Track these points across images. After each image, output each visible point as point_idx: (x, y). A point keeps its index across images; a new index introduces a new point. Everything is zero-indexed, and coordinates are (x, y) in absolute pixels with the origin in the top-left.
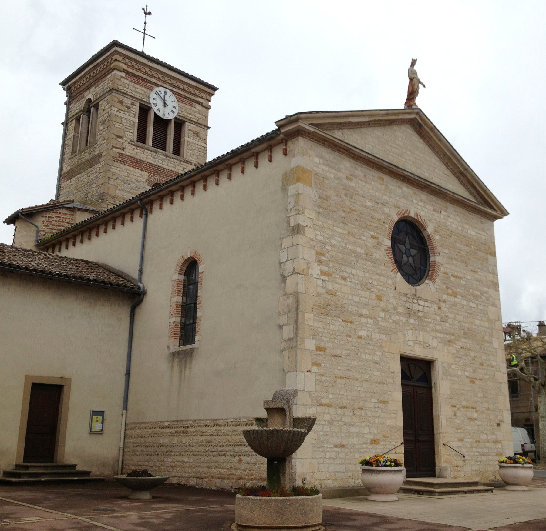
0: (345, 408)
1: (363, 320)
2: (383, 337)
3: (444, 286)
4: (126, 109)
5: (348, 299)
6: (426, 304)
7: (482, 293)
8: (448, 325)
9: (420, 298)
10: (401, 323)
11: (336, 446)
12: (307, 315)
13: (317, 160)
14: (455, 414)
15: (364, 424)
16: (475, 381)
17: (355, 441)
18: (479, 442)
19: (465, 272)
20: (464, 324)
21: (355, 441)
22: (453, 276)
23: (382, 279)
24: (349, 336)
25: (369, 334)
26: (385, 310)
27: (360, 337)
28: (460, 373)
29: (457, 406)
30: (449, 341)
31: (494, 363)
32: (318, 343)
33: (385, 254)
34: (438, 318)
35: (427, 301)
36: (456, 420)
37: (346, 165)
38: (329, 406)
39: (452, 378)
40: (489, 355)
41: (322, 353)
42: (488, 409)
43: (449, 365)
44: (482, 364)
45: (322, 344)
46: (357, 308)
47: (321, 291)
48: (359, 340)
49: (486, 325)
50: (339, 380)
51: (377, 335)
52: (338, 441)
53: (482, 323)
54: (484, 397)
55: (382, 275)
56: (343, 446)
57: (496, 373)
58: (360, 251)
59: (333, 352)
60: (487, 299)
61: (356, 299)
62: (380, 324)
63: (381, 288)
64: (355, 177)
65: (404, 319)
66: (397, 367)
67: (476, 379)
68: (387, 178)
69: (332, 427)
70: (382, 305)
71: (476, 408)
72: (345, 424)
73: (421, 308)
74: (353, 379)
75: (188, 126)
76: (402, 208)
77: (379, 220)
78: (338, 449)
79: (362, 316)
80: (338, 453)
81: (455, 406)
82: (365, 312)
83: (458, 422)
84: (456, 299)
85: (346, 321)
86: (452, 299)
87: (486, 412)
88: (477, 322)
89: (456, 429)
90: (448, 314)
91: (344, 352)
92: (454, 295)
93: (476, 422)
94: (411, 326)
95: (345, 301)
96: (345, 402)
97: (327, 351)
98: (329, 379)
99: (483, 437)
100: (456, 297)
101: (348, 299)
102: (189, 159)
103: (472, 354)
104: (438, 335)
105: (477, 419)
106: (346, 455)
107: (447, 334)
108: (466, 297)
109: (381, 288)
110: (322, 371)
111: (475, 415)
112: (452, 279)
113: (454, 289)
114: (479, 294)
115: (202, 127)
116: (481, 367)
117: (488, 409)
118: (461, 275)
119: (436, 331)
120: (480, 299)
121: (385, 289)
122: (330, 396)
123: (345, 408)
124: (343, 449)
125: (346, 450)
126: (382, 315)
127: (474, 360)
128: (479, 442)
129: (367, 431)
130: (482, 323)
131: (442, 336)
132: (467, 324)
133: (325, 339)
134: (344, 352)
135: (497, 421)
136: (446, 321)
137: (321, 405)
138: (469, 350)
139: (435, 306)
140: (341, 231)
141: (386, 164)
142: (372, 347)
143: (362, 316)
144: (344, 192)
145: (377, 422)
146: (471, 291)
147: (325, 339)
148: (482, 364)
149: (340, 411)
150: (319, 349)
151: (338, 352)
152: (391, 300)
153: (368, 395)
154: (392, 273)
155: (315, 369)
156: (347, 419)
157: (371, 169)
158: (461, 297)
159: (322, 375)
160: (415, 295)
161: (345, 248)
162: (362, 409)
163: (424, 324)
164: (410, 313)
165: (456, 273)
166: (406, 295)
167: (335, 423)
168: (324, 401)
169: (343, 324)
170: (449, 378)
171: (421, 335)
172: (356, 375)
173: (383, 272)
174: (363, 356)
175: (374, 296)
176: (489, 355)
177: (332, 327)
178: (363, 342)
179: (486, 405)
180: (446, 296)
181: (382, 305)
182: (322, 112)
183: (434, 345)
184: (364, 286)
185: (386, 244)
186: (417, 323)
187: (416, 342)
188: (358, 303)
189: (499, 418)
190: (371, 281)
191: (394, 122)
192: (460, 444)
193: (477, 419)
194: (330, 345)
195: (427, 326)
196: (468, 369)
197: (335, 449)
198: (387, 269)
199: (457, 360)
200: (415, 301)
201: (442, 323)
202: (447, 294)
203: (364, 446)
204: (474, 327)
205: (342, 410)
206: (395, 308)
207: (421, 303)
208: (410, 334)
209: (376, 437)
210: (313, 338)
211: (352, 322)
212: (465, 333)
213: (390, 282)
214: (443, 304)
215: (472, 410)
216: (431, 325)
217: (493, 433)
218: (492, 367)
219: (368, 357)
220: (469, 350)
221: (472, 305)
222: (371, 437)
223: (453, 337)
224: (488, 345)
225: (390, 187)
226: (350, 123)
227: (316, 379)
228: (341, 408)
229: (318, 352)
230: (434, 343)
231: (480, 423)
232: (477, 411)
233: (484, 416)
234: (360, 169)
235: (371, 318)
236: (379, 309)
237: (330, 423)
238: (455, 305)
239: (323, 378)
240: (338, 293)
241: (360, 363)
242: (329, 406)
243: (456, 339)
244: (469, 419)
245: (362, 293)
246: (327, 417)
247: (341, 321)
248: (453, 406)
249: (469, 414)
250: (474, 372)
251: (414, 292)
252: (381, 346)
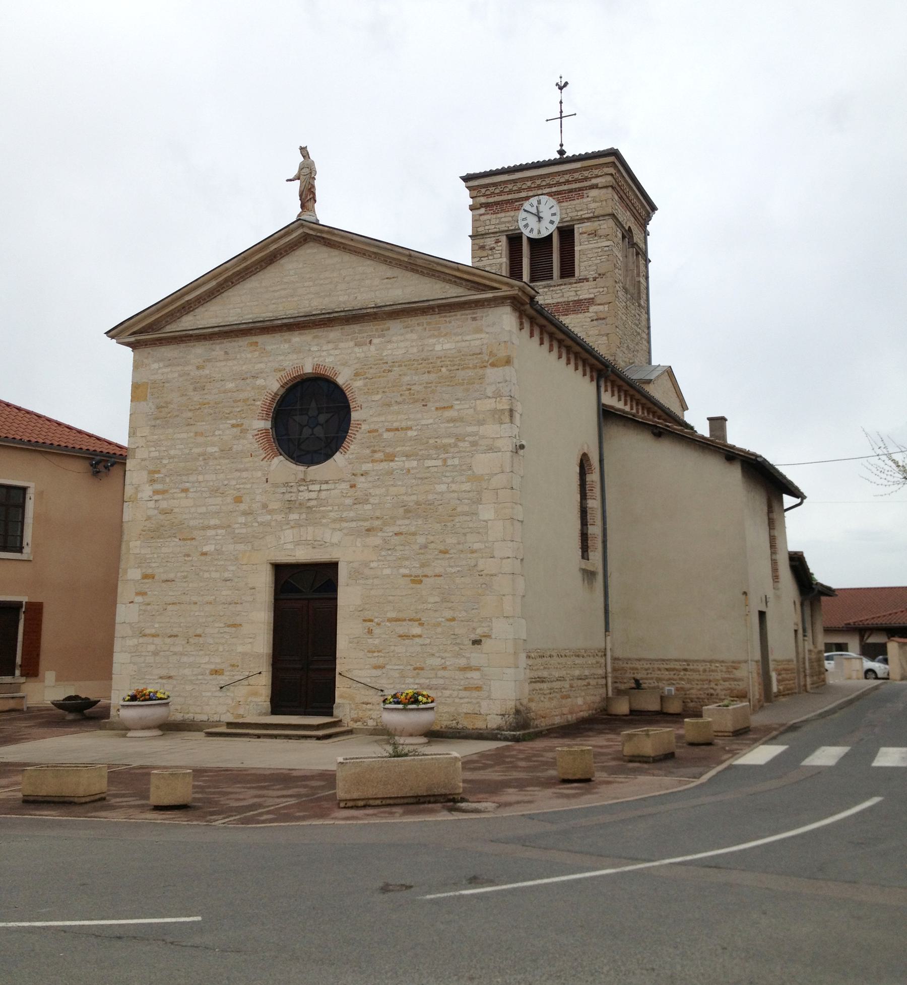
0: (176, 636)
1: (210, 533)
2: (241, 547)
3: (368, 451)
4: (490, 252)
5: (190, 513)
6: (324, 487)
7: (459, 438)
8: (369, 507)
9: (313, 482)
10: (273, 524)
11: (161, 678)
12: (132, 544)
13: (156, 366)
14: (370, 632)
15: (202, 652)
16: (424, 579)
17: (187, 671)
18: (422, 669)
19: (419, 416)
20: (405, 498)
21: (187, 671)
22: (388, 430)
23: (245, 474)
24: (188, 556)
25: (218, 547)
26: (245, 513)
27: (204, 554)
28: (387, 571)
29: (376, 620)
30: (368, 530)
31: (476, 546)
32: (144, 570)
33: (254, 440)
34: (348, 501)
35: (327, 482)
36: (370, 641)
37: (198, 351)
38: (154, 636)
39: (370, 581)
40: (465, 534)
41: (150, 580)
42: (453, 619)
43: (366, 564)
44: (445, 552)
45: (150, 571)
46: (201, 521)
47: (151, 512)
48: (203, 558)
49: (466, 487)
50: (170, 607)
51: (231, 547)
52: (164, 672)
53: (454, 487)
54: (444, 600)
55: (246, 470)
56: (170, 677)
57: (481, 563)
58: (210, 450)
59: (165, 577)
60: (474, 444)
61: (203, 510)
62: (237, 531)
63: (242, 486)
64: (209, 361)
65: (279, 517)
66: (264, 582)
67: (426, 576)
68: (261, 339)
69: (157, 658)
70: (243, 507)
71: (420, 620)
72: (175, 654)
73: (313, 495)
74: (190, 603)
75: (578, 229)
76: (287, 369)
77: (245, 401)
78: (164, 681)
79: (209, 527)
80: (164, 684)
81: (371, 621)
82: (213, 522)
83: (377, 642)
84: (392, 464)
85: (184, 539)
86: (385, 465)
87: (448, 624)
88: (442, 488)
89: (369, 651)
90: (371, 491)
91: (179, 574)
92: (390, 458)
93: (417, 640)
94: (292, 523)
95: (185, 516)
96: (175, 629)
97: (156, 577)
98: (156, 607)
99: (436, 662)
100: (392, 461)
101: (190, 513)
102: (584, 274)
103: (421, 540)
104: (345, 525)
105: (420, 636)
106: (175, 687)
107: (366, 520)
108: (417, 455)
109: (242, 486)
110: (147, 600)
111: (417, 630)
112: (386, 435)
113: (388, 450)
114: (452, 441)
115: (601, 218)
116: (441, 556)
117: (453, 619)
118: (409, 423)
119: (342, 520)
120: (452, 450)
121: (249, 486)
122: (157, 625)
123: (176, 636)
124: (170, 681)
125: (175, 682)
126: (242, 519)
127: (426, 547)
128: (422, 669)
129: (206, 659)
130: (454, 487)
131: (354, 524)
132: (414, 498)
133: (154, 565)
134: (179, 574)
135: (473, 637)
136: (366, 502)
137: (145, 635)
138: (414, 534)
139: (344, 486)
140: (184, 435)
141: (244, 326)
142: (222, 563)
143: (209, 527)
144: (192, 387)
145: (221, 649)
146: (431, 441)
147: (154, 565)
148: (445, 552)
149: (168, 640)
150: (145, 576)
151: (171, 576)
152: (258, 498)
153: (210, 619)
154: (264, 462)
155: (139, 599)
156: (178, 649)
157: (236, 339)
158: (404, 458)
159: (149, 604)
160: (304, 480)
161: (188, 454)
162: (200, 636)
163: (318, 515)
164: (291, 506)
165: (396, 425)
166: (286, 484)
167: (162, 653)
168: (147, 631)
169: (182, 543)
170: (361, 581)
171: (310, 533)
172: (194, 599)
173: (248, 465)
174: (206, 575)
175: (229, 500)
176: (465, 534)
177: (164, 550)
178: (208, 558)
179: (448, 614)
180: (370, 465)
181: (243, 507)
182: (137, 315)
183: (335, 540)
184: (215, 491)
185: (254, 427)
186: (304, 516)
187: (297, 544)
188: (204, 514)
189: (479, 631)
190: (226, 482)
191: (275, 257)
192: (378, 672)
193: (420, 636)
194: (161, 570)
195: (324, 517)
196: (407, 563)
197: (160, 680)
198: (256, 459)
199: (383, 553)
200: (302, 488)
201: (355, 506)
202: (373, 461)
203: (200, 677)
204: (430, 497)
205: (172, 638)
206: (265, 506)
207: (317, 487)
208: (289, 535)
209: (218, 667)
210: (139, 567)
211: (193, 539)
212: (407, 511)
213: (259, 474)
214: (362, 479)
215: (410, 623)
216: (332, 514)
217: (458, 655)
218: (473, 552)
219: (215, 575)
220: (414, 534)
221: (429, 463)
222: (212, 667)
223: (377, 523)
224: (468, 518)
225: (269, 348)
226: (189, 302)
227: (140, 610)
228: (170, 636)
229: (146, 581)
230: (335, 539)
231: (428, 641)
232: (421, 624)
233: (439, 630)
234: (218, 347)
235: (223, 528)
236: (235, 514)
237: (155, 654)
238: (390, 473)
239: (149, 607)
240: (176, 510)
241: (201, 584)
242: (154, 636)
243: (385, 524)
244: (400, 636)
245: (210, 501)
246: (151, 648)
247: (177, 540)
248: (364, 621)
249: (402, 629)
250: (423, 565)
251: (301, 476)
252: (237, 559)
